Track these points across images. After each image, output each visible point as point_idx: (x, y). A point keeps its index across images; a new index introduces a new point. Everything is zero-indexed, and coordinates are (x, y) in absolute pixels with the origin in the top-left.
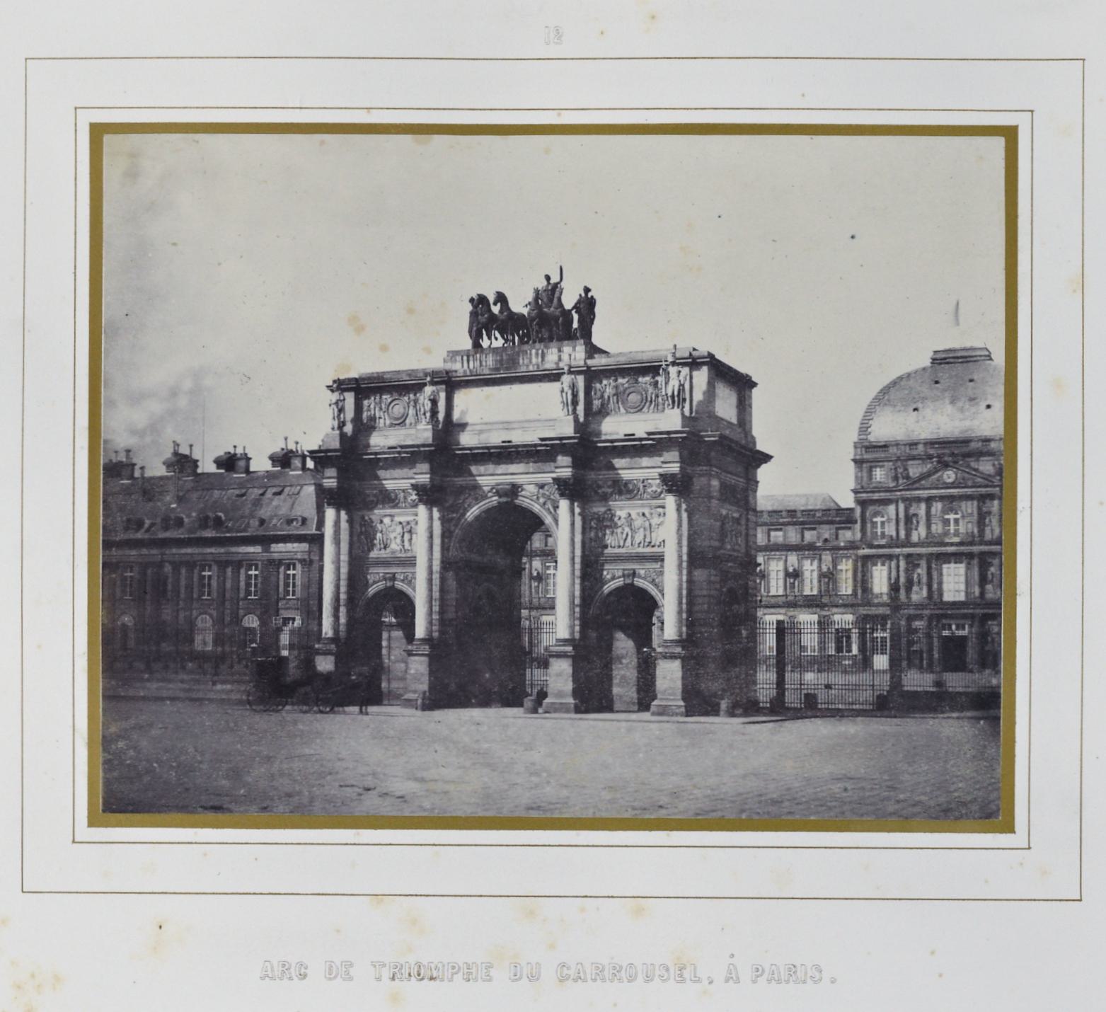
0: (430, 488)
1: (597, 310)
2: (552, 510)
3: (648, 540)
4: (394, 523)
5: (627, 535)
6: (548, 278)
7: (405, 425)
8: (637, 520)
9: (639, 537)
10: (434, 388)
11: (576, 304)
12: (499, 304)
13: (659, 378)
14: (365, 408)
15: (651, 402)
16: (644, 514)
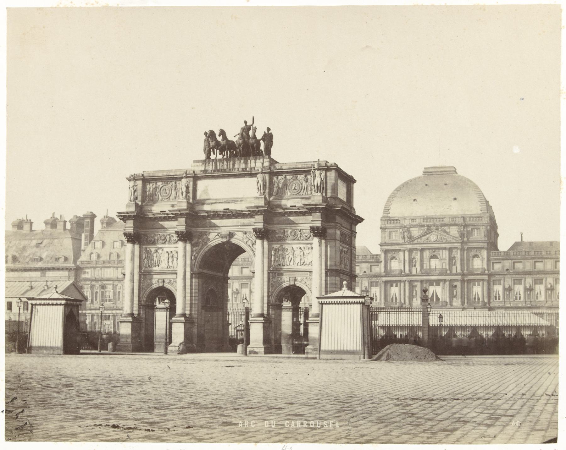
0: (186, 233)
1: (274, 140)
2: (251, 245)
3: (302, 261)
4: (163, 252)
5: (291, 259)
6: (246, 122)
7: (170, 199)
8: (296, 251)
9: (298, 260)
10: (187, 179)
11: (263, 137)
12: (222, 136)
13: (309, 177)
14: (148, 190)
15: (304, 189)
16: (300, 248)
